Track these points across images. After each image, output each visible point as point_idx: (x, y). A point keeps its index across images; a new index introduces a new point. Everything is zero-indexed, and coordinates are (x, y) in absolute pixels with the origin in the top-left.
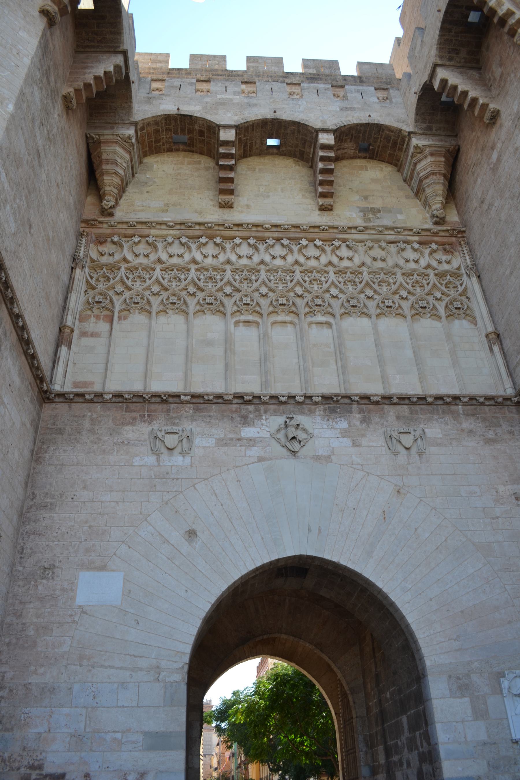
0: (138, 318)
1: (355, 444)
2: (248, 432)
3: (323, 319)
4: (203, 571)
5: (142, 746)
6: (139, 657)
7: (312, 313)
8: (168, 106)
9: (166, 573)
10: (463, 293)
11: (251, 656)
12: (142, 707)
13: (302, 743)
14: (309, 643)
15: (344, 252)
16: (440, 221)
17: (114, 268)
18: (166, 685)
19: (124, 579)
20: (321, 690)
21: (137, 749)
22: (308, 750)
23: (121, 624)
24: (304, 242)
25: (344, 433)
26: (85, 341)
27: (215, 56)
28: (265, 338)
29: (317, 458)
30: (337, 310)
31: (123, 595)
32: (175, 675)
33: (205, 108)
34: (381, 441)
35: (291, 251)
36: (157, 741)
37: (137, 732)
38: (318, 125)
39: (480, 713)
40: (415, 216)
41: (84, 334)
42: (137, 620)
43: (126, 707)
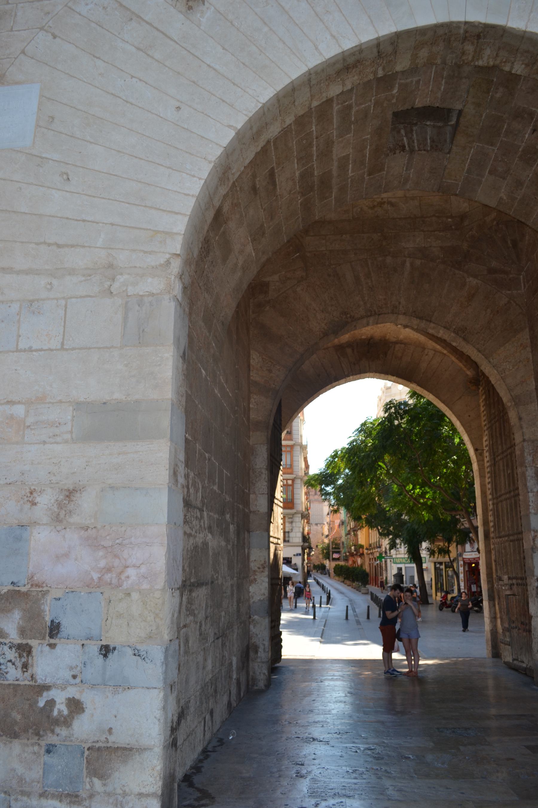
4: (217, 67)
5: (71, 432)
6: (67, 246)
9: (132, 77)
11: (353, 375)
12: (73, 349)
13: (423, 495)
14: (445, 327)
18: (127, 303)
19: (42, 96)
20: (454, 419)
21: (58, 439)
22: (431, 503)
23: (32, 184)
31: (38, 126)
32: (150, 280)
37: (61, 402)
42: (67, 174)
43: (36, 350)
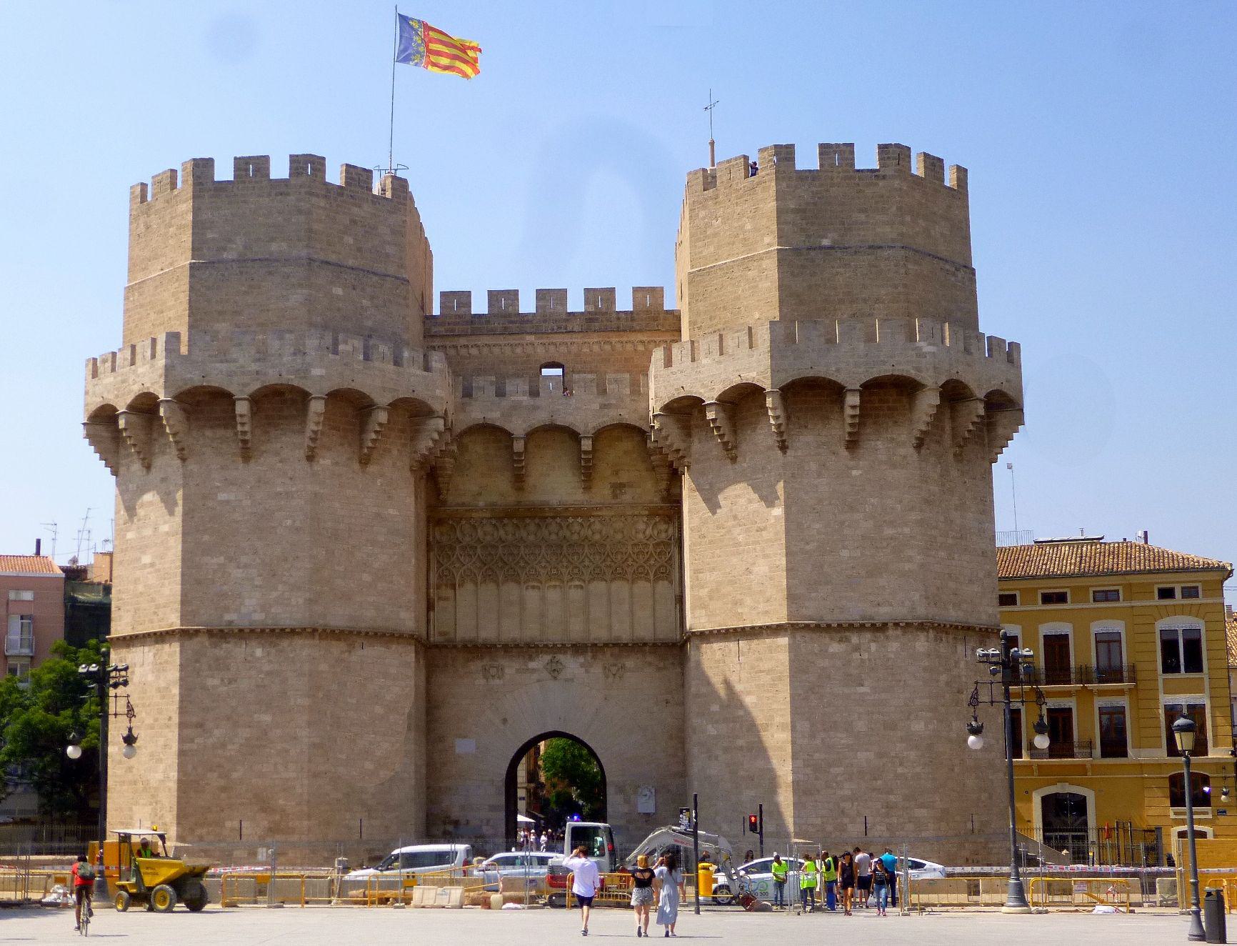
0: (469, 586)
1: (587, 672)
2: (532, 665)
3: (577, 583)
7: (572, 580)
8: (477, 413)
10: (670, 559)
15: (597, 526)
16: (664, 500)
17: (452, 548)
24: (571, 520)
25: (582, 665)
26: (441, 603)
27: (508, 291)
28: (543, 599)
29: (566, 680)
30: (587, 577)
33: (503, 415)
34: (601, 670)
35: (561, 527)
36: (493, 808)
38: (580, 428)
39: (627, 801)
40: (648, 491)
41: (440, 598)
